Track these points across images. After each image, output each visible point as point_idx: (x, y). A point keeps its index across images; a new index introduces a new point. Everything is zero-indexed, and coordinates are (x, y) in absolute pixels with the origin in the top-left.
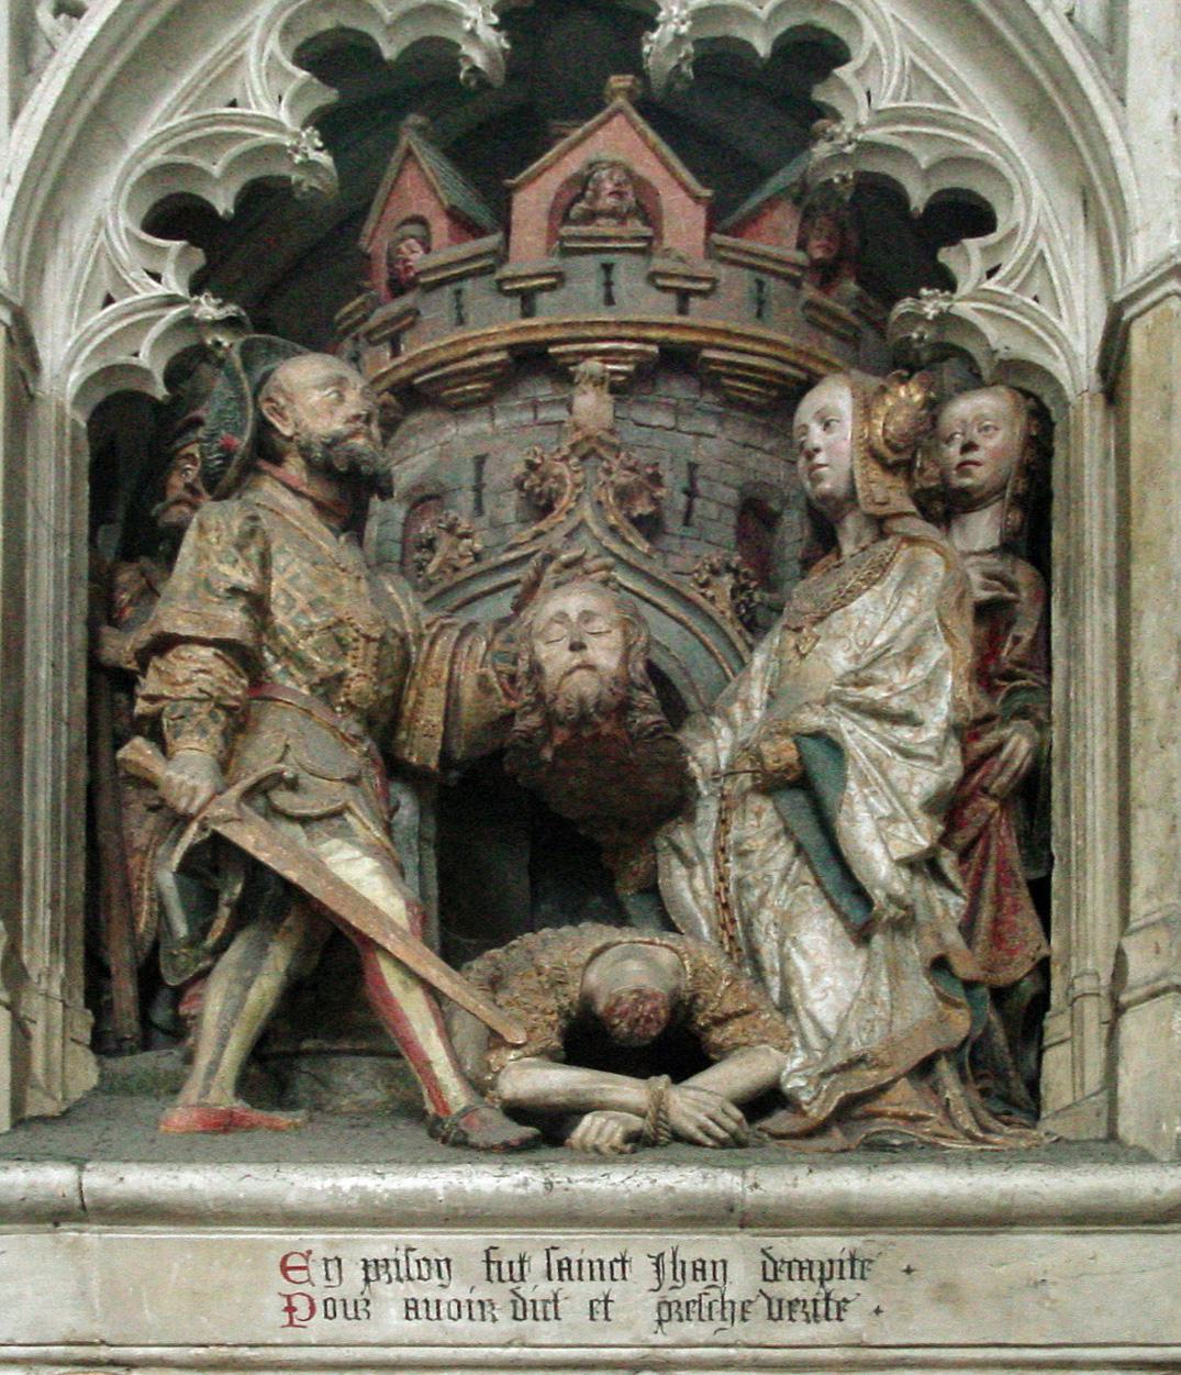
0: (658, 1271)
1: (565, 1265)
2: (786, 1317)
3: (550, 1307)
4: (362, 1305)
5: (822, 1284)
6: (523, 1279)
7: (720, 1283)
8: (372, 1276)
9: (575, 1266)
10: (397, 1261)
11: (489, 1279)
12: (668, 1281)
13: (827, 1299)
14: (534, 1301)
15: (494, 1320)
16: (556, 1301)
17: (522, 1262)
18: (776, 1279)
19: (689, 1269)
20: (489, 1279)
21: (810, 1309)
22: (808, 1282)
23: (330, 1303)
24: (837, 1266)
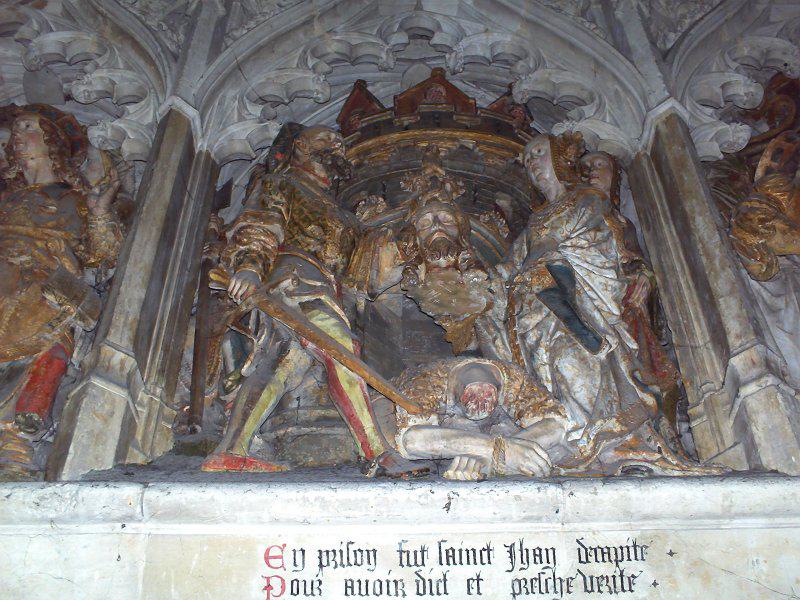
0: (511, 557)
1: (451, 553)
2: (596, 589)
3: (441, 585)
4: (316, 584)
5: (617, 565)
6: (423, 564)
7: (551, 565)
8: (324, 563)
9: (457, 553)
10: (341, 551)
11: (401, 565)
12: (518, 563)
13: (622, 576)
14: (430, 581)
15: (404, 595)
16: (445, 580)
17: (423, 551)
18: (588, 561)
19: (531, 553)
20: (401, 565)
21: (611, 583)
22: (608, 563)
23: (295, 583)
24: (625, 550)
